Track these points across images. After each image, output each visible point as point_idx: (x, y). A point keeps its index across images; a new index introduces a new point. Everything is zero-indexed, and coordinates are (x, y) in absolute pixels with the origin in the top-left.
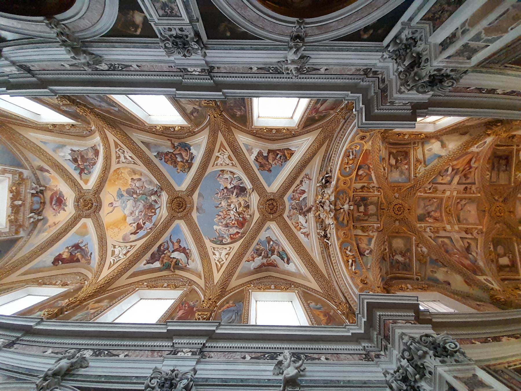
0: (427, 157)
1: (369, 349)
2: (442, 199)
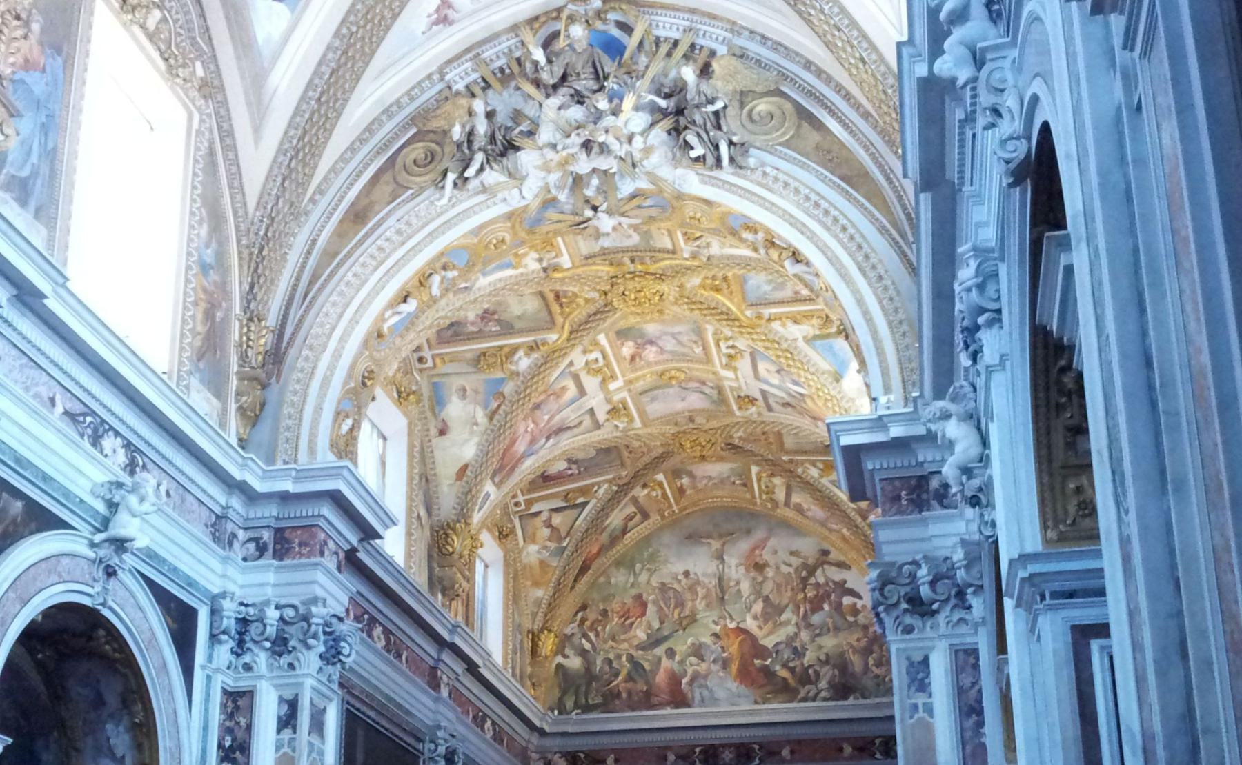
1: (231, 514)
2: (708, 360)
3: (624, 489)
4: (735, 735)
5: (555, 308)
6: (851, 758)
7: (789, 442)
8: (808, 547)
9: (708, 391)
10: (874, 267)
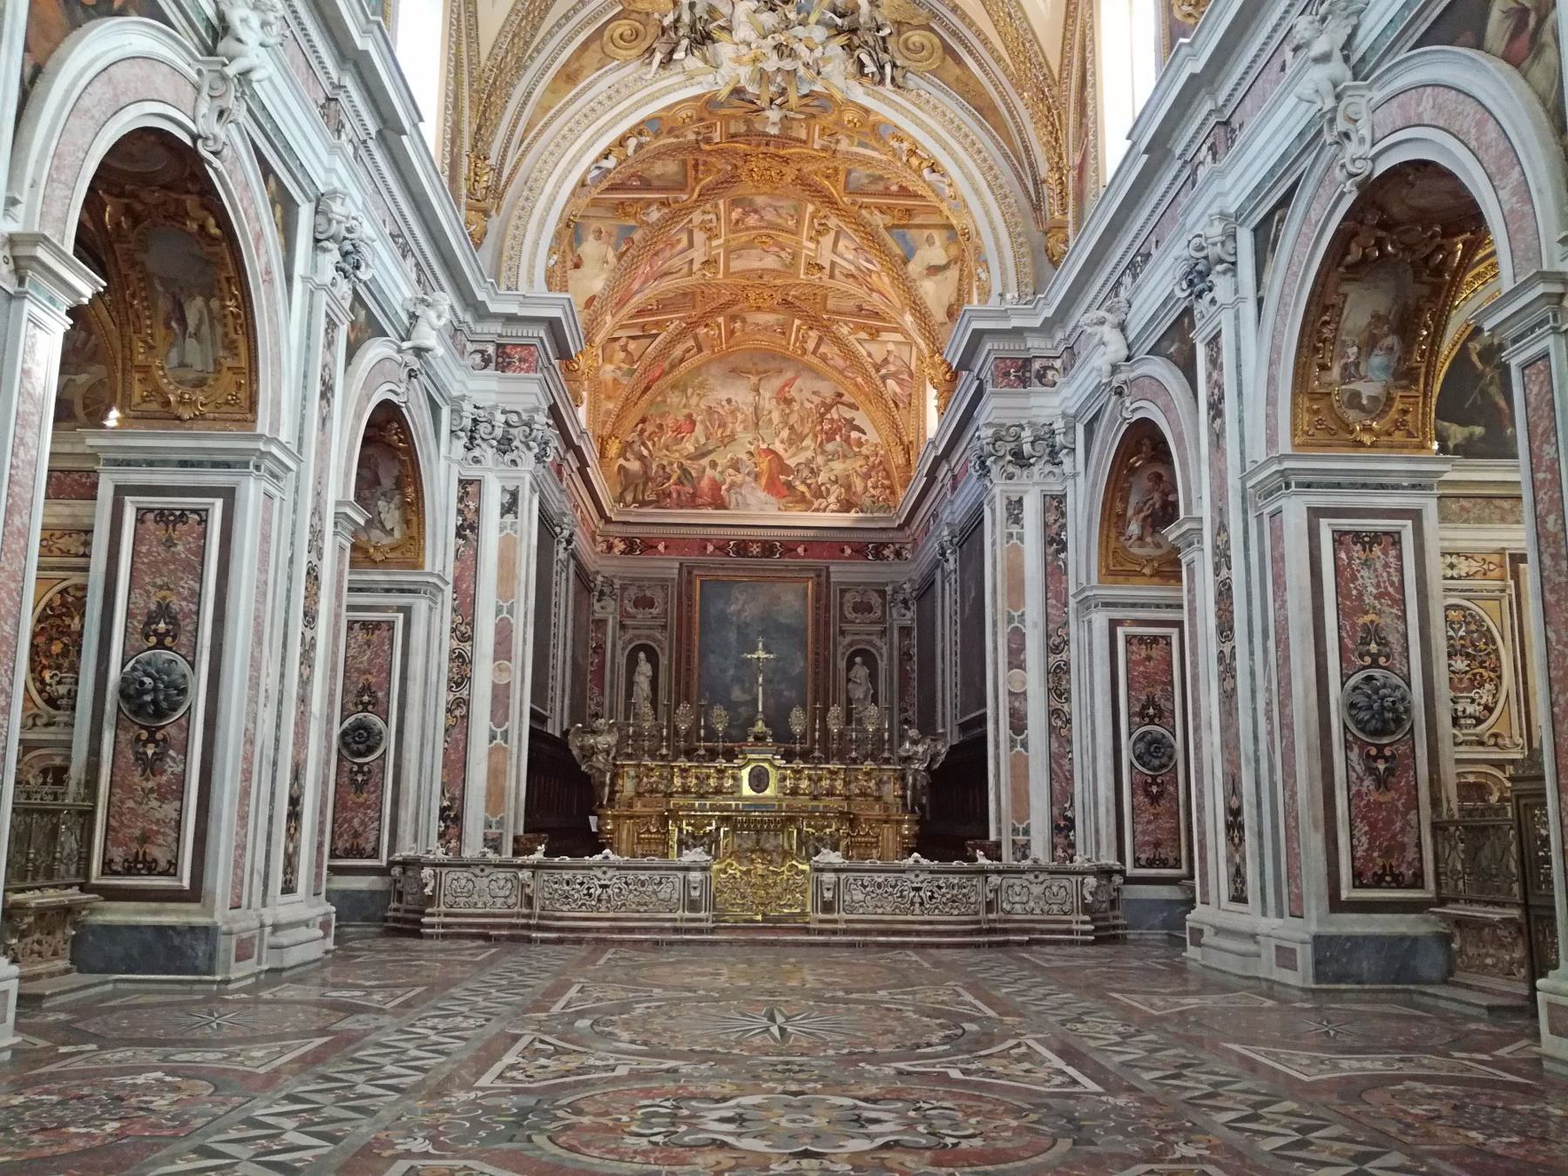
0: (913, 232)
2: (794, 233)
3: (692, 325)
4: (855, 536)
5: (691, 173)
6: (850, 557)
7: (831, 304)
8: (827, 390)
9: (783, 254)
10: (1001, 187)
